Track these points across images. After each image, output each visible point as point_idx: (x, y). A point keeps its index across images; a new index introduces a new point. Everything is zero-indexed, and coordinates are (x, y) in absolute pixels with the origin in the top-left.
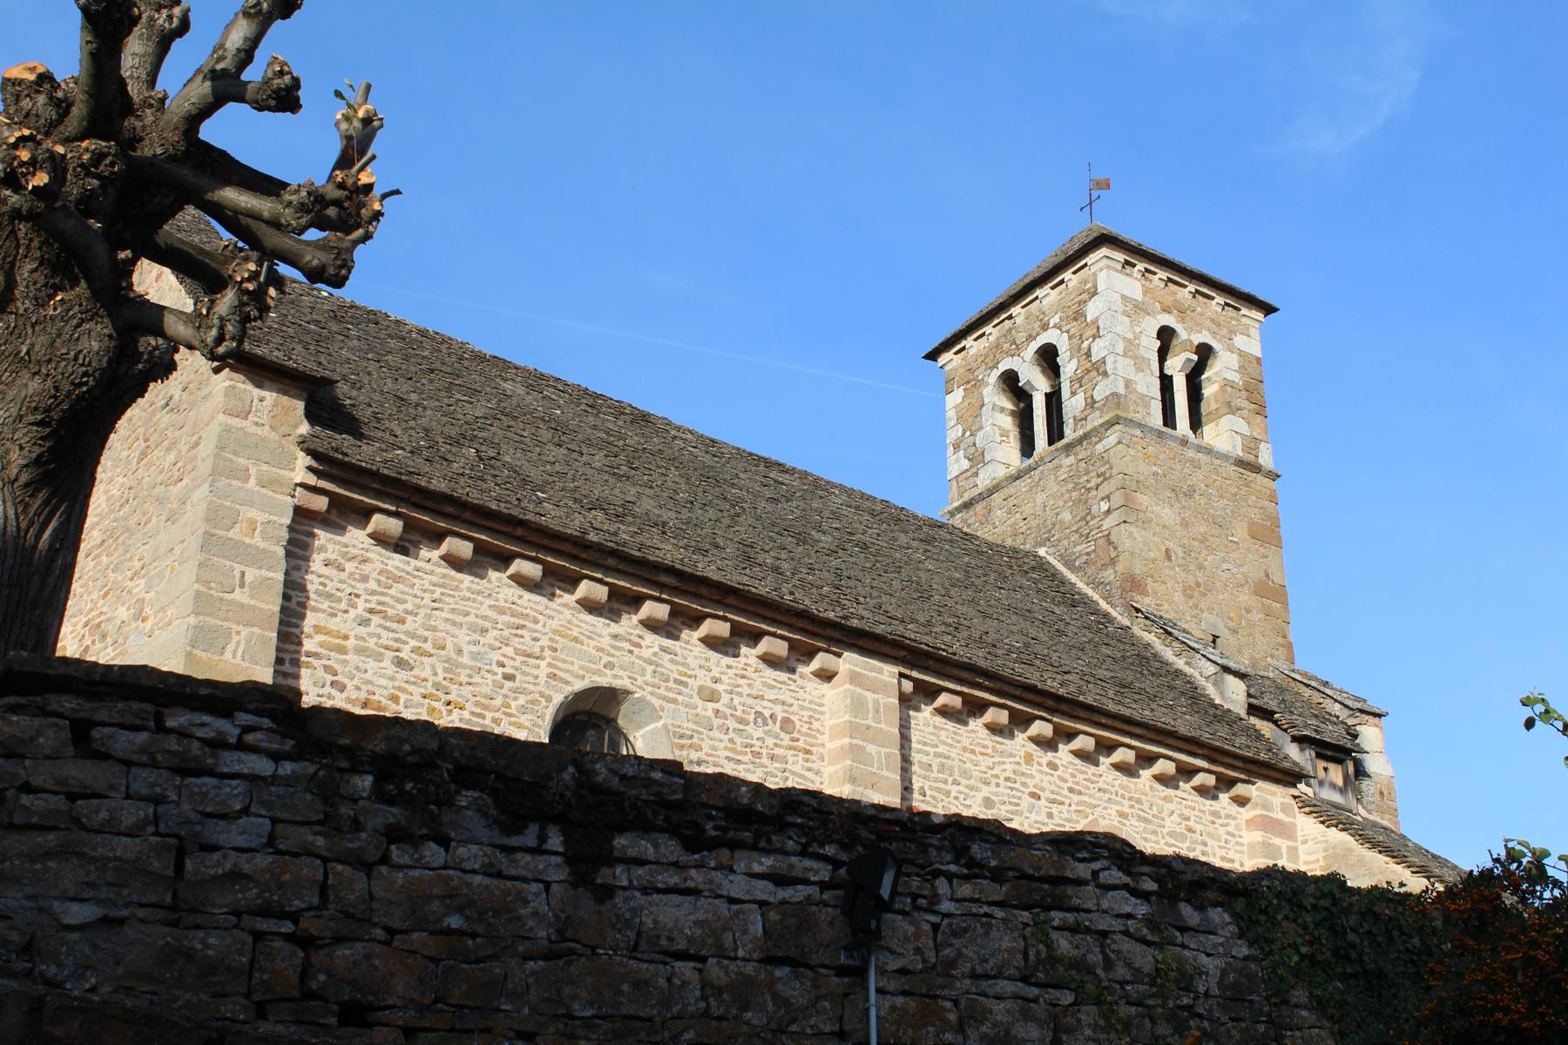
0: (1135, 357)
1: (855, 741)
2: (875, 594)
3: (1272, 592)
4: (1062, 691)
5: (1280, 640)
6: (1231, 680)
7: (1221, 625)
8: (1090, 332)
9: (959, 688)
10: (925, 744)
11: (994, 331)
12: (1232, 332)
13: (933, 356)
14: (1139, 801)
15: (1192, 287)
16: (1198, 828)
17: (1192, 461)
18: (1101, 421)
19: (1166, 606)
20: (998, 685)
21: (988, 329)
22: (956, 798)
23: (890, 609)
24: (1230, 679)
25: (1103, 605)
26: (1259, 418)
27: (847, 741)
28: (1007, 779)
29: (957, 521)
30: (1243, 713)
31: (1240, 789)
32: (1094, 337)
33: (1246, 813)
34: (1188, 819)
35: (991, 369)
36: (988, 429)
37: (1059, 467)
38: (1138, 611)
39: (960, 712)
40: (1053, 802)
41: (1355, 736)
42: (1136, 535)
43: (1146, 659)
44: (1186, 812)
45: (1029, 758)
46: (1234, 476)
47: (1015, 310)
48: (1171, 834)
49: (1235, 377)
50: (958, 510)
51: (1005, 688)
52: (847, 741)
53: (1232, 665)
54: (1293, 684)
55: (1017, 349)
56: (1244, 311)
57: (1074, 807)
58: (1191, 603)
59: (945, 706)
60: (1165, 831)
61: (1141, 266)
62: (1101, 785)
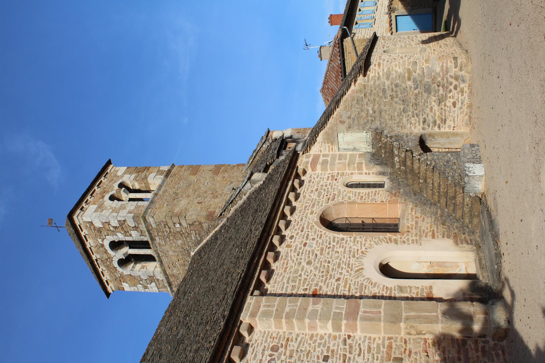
0: (120, 209)
1: (284, 316)
2: (211, 307)
3: (217, 169)
4: (261, 229)
5: (236, 168)
6: (253, 178)
7: (229, 187)
8: (107, 227)
9: (258, 271)
10: (283, 288)
11: (101, 267)
12: (116, 176)
13: (108, 294)
14: (306, 207)
15: (96, 188)
16: (316, 187)
17: (163, 192)
18: (143, 224)
19: (220, 205)
20: (258, 254)
21: (100, 270)
22: (307, 276)
23: (219, 300)
24: (253, 178)
25: (217, 229)
26: (150, 169)
27: (283, 320)
28: (298, 255)
29: (175, 289)
30: (265, 175)
31: (300, 171)
32: (109, 224)
33: (309, 171)
34: (312, 191)
35: (116, 270)
36: (140, 273)
37: (159, 244)
38: (221, 214)
39: (268, 272)
40: (307, 238)
41: (276, 139)
42: (191, 214)
43: (243, 209)
44: (309, 191)
45: (288, 246)
46: (171, 179)
47: (94, 258)
48: (319, 196)
49: (133, 176)
50: (171, 288)
51: (259, 251)
52: (283, 320)
53: (248, 176)
54: (253, 163)
55: (110, 258)
56: (108, 171)
57: (309, 230)
58: (219, 196)
59: (266, 278)
60: (317, 198)
61: (84, 204)
62: (299, 220)
